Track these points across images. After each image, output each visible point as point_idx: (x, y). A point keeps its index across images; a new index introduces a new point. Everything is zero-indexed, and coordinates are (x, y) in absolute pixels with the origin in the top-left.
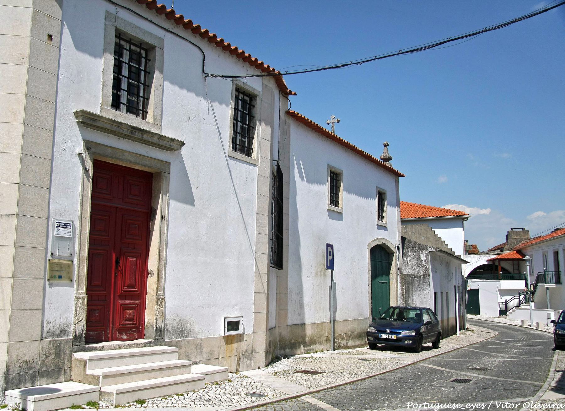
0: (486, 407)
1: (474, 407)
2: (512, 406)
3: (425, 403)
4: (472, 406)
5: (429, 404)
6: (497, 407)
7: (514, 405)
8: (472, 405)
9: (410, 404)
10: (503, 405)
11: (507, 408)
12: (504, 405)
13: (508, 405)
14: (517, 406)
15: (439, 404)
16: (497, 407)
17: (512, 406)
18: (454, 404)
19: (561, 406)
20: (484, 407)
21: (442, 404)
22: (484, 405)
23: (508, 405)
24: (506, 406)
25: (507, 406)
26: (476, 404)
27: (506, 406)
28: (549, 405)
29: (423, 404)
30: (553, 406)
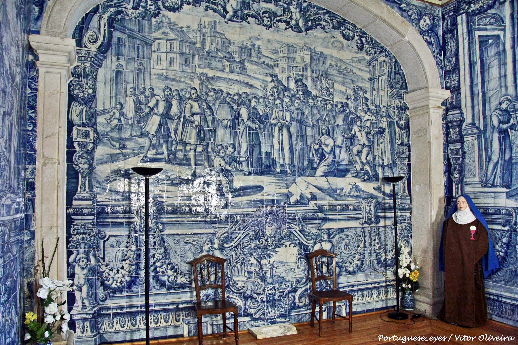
0: (447, 340)
2: (469, 339)
3: (394, 336)
6: (456, 340)
9: (381, 337)
12: (462, 338)
13: (466, 338)
14: (473, 338)
16: (456, 340)
17: (469, 339)
19: (511, 339)
23: (466, 338)
24: (464, 339)
27: (464, 339)
30: (505, 338)
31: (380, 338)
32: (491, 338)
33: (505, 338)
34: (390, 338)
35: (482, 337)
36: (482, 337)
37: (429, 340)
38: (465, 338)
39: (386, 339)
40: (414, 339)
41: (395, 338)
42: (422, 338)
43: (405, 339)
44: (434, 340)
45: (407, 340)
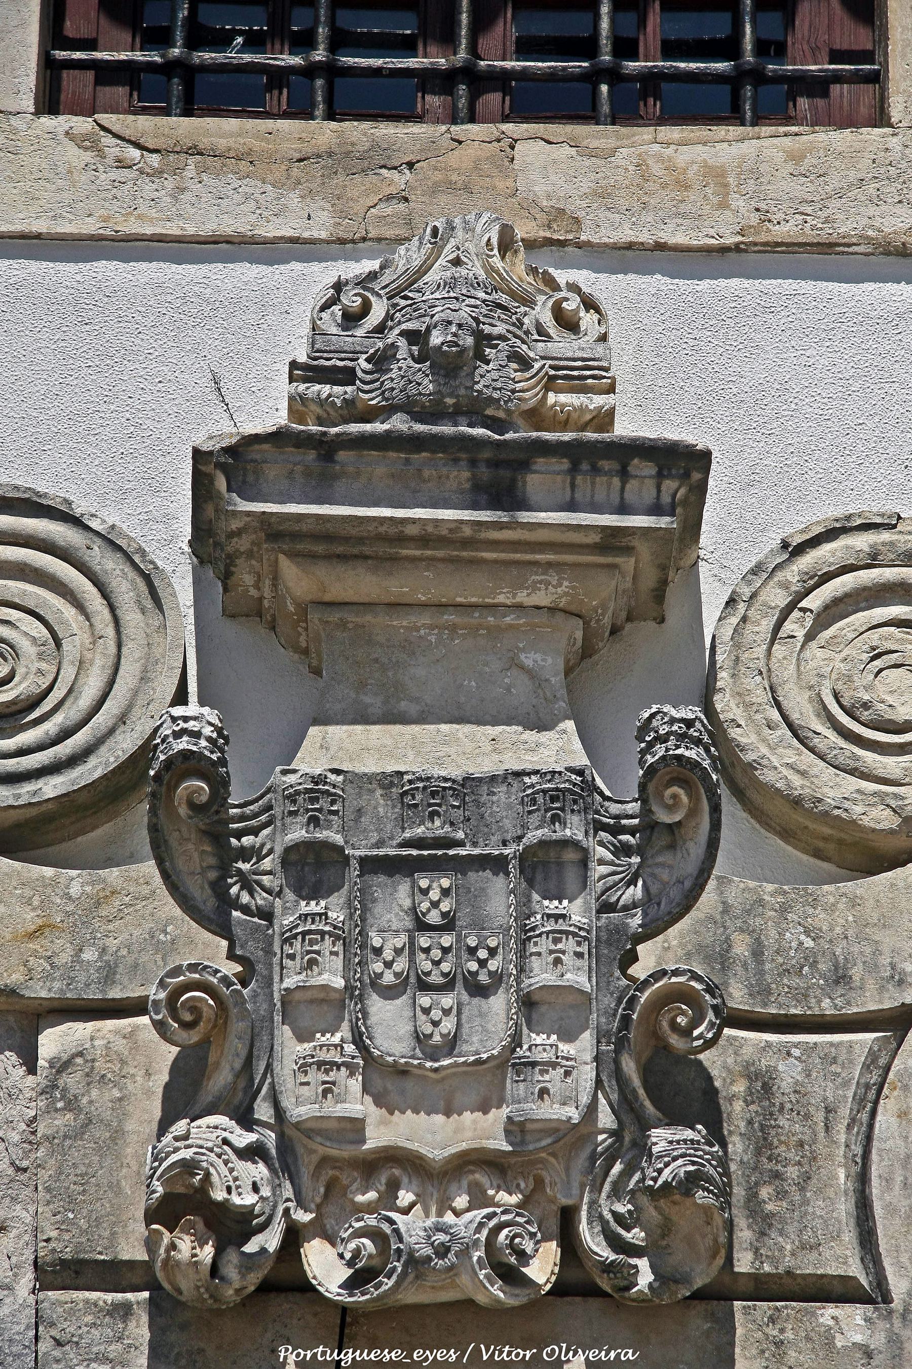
1: (431, 1358)
2: (517, 1355)
3: (321, 1348)
5: (329, 1352)
6: (485, 1358)
7: (522, 1353)
8: (428, 1352)
9: (287, 1350)
10: (497, 1352)
11: (506, 1359)
12: (501, 1352)
15: (351, 1351)
16: (485, 1358)
17: (517, 1355)
18: (387, 1350)
19: (630, 1355)
20: (454, 1357)
21: (359, 1351)
22: (455, 1353)
24: (505, 1355)
25: (508, 1357)
26: (435, 1351)
27: (505, 1355)
28: (603, 1353)
29: (315, 1351)
30: (612, 1355)
33: (612, 1355)
34: (309, 1354)
35: (553, 1350)
36: (553, 1350)
37: (412, 1358)
38: (506, 1354)
40: (372, 1356)
41: (324, 1353)
42: (393, 1354)
44: (427, 1358)
45: (354, 1359)
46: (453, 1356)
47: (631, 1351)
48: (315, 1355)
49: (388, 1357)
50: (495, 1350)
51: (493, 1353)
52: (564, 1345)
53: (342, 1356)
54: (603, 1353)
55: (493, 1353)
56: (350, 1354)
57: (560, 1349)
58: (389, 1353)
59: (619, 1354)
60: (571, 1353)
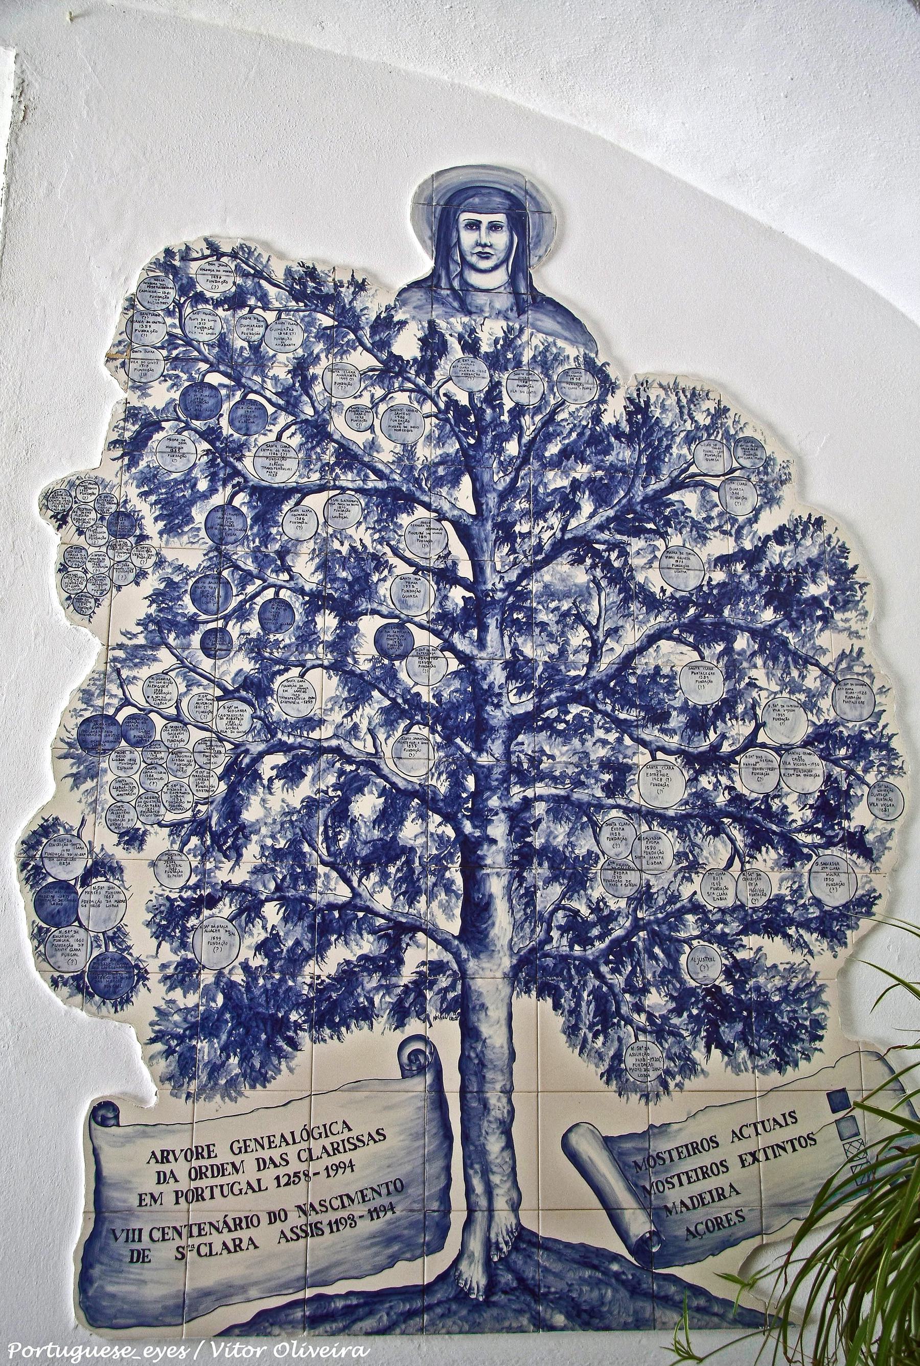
1: (161, 1355)
2: (248, 1352)
3: (50, 1346)
4: (157, 1355)
6: (215, 1355)
7: (252, 1350)
8: (158, 1349)
12: (231, 1350)
15: (80, 1348)
16: (215, 1355)
17: (248, 1352)
19: (361, 1352)
20: (184, 1354)
24: (235, 1352)
27: (235, 1352)
28: (334, 1350)
30: (343, 1352)
31: (12, 1351)
32: (306, 1349)
33: (343, 1352)
34: (39, 1351)
35: (284, 1347)
37: (141, 1355)
39: (28, 1352)
40: (102, 1353)
41: (53, 1351)
42: (123, 1351)
43: (80, 1353)
44: (157, 1355)
45: (83, 1356)
46: (183, 1352)
47: (362, 1348)
48: (45, 1351)
49: (118, 1354)
50: (225, 1346)
51: (224, 1349)
52: (295, 1342)
53: (72, 1353)
54: (334, 1350)
55: (224, 1349)
56: (80, 1352)
57: (291, 1345)
58: (119, 1350)
59: (350, 1351)
60: (302, 1350)
